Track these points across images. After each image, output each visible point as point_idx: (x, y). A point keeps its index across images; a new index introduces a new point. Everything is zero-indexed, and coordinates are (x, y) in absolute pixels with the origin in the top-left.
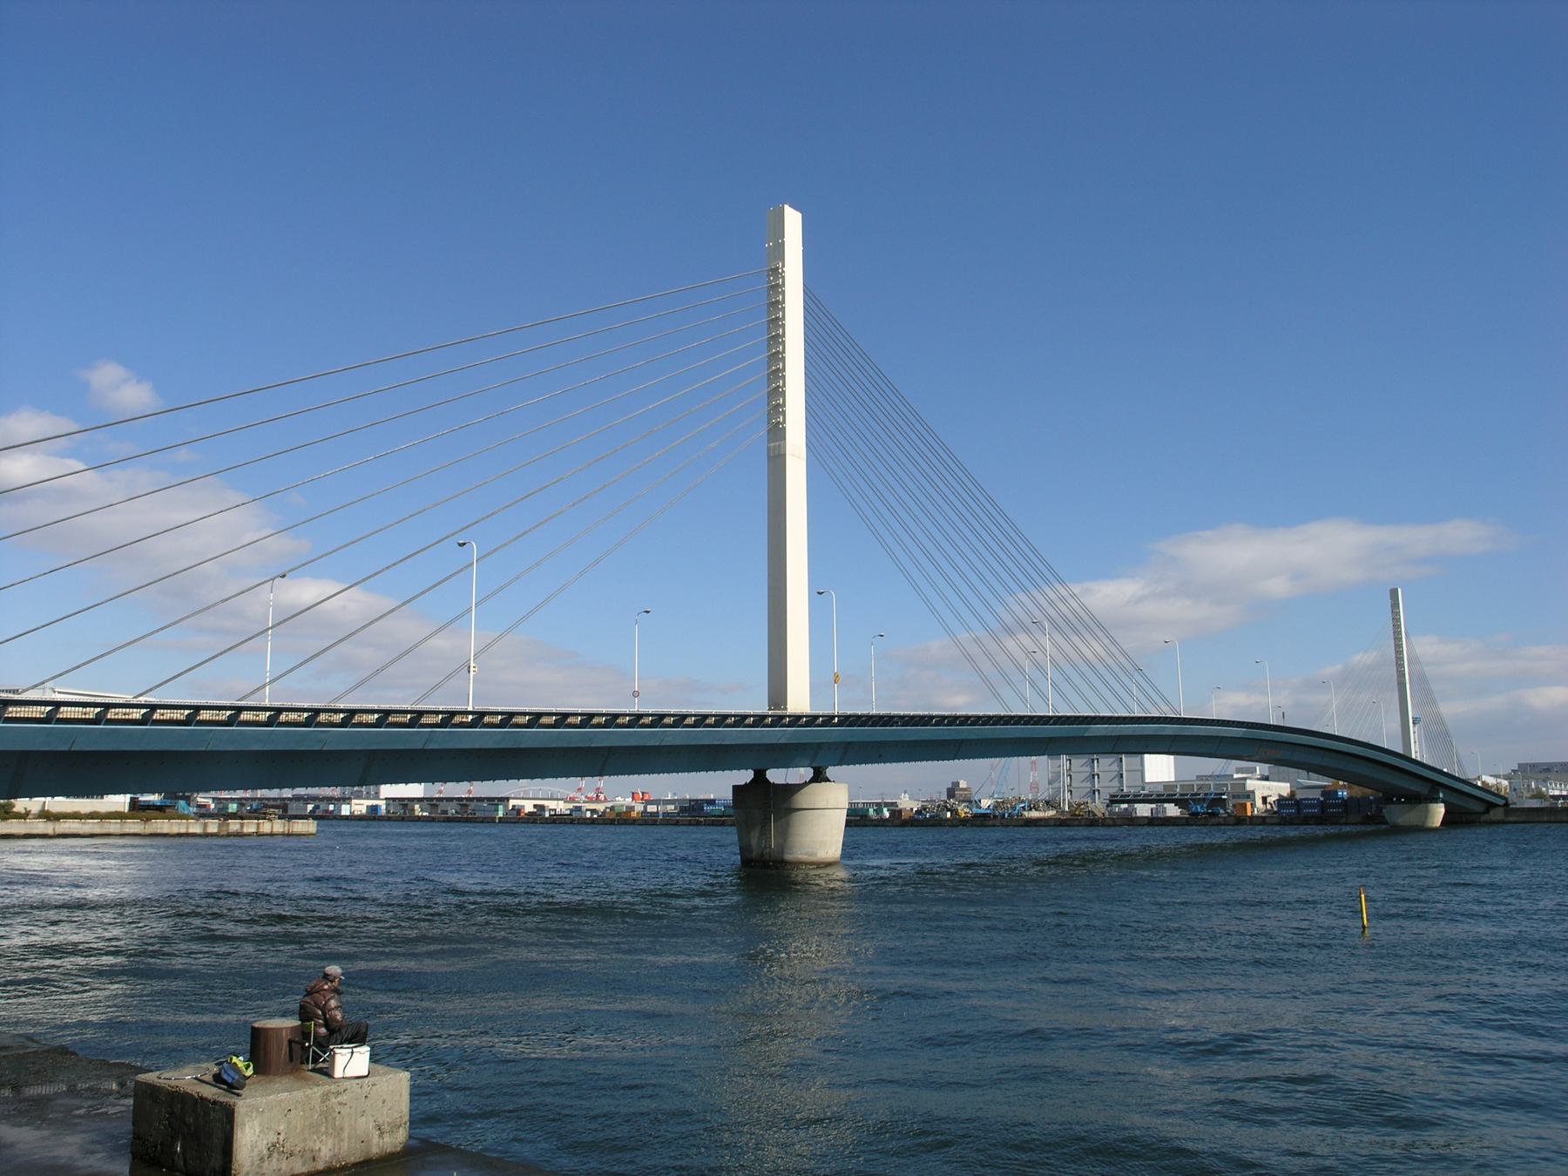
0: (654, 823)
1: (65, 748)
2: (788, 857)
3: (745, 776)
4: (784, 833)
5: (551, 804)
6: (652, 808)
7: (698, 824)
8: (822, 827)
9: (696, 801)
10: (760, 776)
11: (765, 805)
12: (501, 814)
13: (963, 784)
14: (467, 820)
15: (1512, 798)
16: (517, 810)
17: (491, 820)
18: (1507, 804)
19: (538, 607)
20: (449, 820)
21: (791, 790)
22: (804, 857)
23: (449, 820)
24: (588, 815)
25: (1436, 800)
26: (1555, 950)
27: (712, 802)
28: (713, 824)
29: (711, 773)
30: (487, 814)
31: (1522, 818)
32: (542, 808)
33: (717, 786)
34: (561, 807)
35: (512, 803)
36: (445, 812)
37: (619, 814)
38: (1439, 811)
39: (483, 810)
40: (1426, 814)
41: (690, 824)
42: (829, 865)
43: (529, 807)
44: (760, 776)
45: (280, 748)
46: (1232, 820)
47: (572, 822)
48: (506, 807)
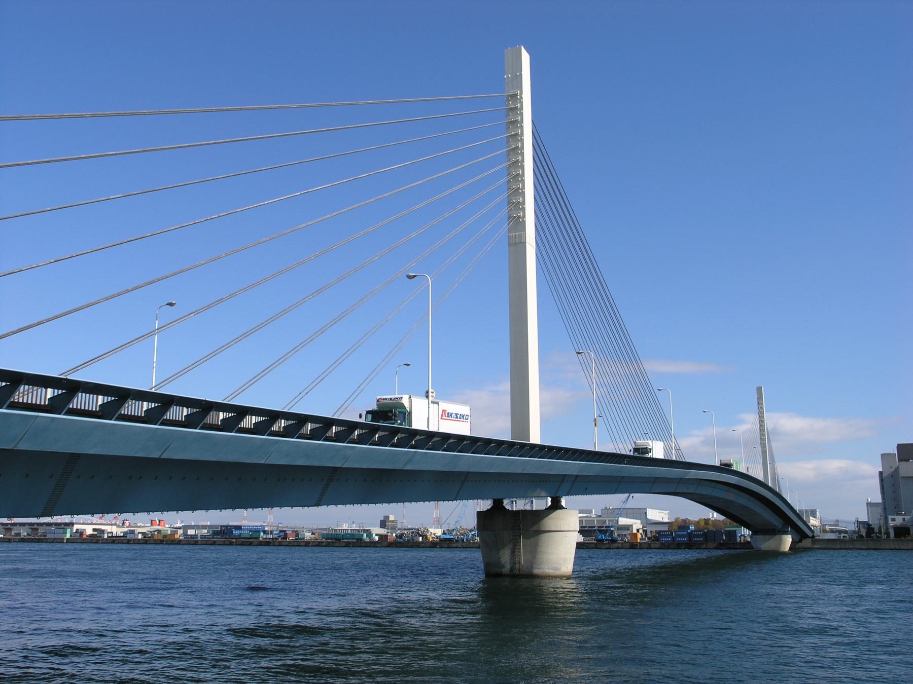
0: (196, 543)
1: (155, 455)
2: (536, 571)
3: (485, 505)
4: (534, 551)
5: (108, 528)
6: (191, 532)
7: (231, 544)
8: (560, 550)
9: (227, 527)
10: (498, 503)
11: (510, 529)
12: (68, 536)
13: (392, 518)
14: (39, 541)
15: (817, 532)
16: (81, 533)
17: (61, 541)
18: (813, 537)
19: (294, 350)
20: (23, 540)
21: (539, 515)
22: (551, 572)
23: (23, 540)
24: (140, 536)
25: (786, 533)
26: (822, 631)
27: (238, 528)
28: (243, 544)
29: (349, 507)
30: (57, 536)
31: (823, 546)
32: (103, 531)
33: (459, 515)
34: (116, 531)
35: (76, 527)
36: (19, 534)
37: (165, 536)
38: (787, 541)
39: (52, 533)
40: (780, 542)
41: (224, 544)
42: (561, 577)
43: (89, 530)
44: (498, 503)
45: (316, 463)
46: (627, 545)
47: (128, 542)
48: (72, 530)
